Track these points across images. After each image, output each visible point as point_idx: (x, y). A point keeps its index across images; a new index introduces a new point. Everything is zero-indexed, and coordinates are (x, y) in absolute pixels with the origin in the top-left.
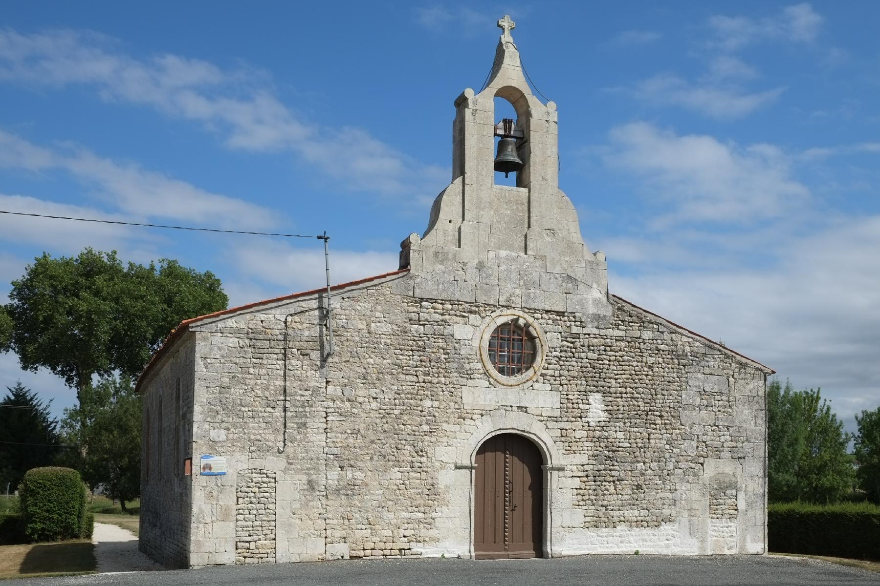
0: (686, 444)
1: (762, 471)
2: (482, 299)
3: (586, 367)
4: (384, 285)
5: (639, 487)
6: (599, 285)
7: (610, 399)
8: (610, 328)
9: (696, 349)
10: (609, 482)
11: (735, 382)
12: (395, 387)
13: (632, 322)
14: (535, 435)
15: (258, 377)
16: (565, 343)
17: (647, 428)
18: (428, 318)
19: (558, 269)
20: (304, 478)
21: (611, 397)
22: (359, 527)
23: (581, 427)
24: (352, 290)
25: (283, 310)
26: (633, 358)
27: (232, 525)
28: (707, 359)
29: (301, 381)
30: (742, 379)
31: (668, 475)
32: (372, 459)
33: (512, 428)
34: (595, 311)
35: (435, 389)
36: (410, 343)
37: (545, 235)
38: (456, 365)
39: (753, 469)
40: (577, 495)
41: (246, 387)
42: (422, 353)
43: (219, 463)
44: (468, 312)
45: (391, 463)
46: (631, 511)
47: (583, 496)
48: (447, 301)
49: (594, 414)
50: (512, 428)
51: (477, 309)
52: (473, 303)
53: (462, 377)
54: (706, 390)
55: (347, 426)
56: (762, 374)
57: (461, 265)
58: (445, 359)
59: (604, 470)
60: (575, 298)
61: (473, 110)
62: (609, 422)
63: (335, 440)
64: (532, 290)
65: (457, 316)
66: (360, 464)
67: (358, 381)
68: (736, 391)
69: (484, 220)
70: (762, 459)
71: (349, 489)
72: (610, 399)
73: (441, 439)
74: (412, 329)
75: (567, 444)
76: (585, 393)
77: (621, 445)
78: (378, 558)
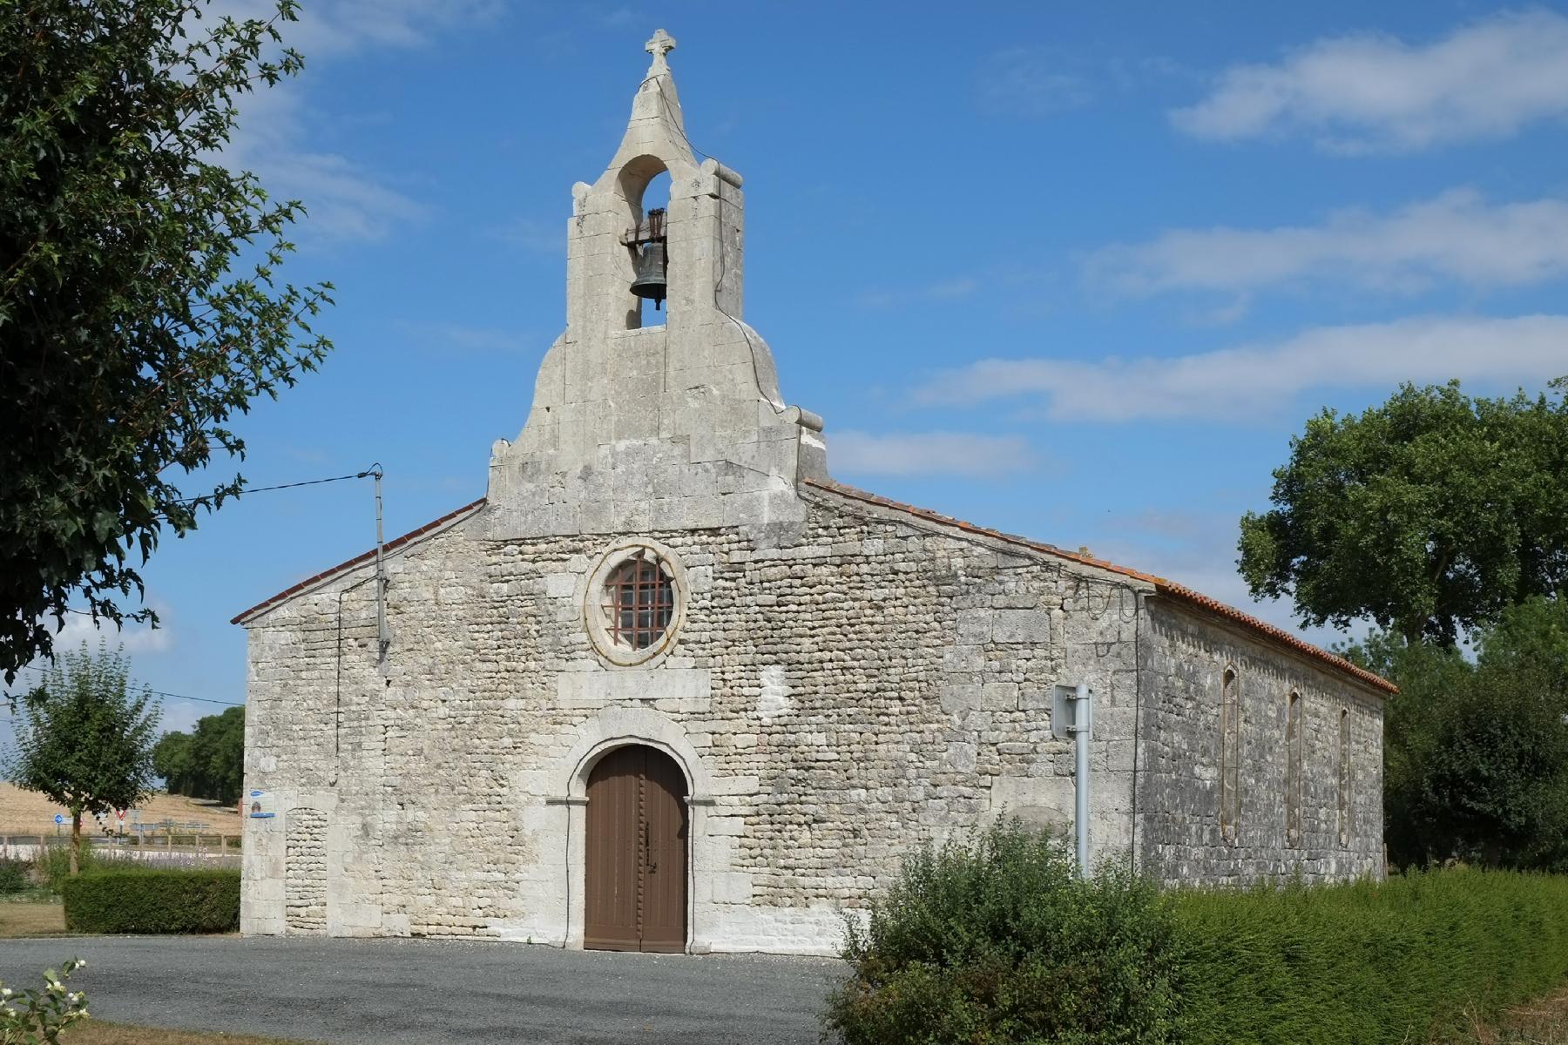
0: (951, 751)
1: (1128, 799)
2: (589, 527)
3: (755, 621)
4: (455, 528)
5: (856, 833)
6: (781, 470)
7: (800, 674)
8: (802, 545)
9: (975, 562)
10: (800, 825)
11: (1066, 619)
12: (468, 682)
13: (845, 527)
14: (668, 745)
15: (309, 683)
16: (721, 583)
17: (872, 724)
18: (513, 570)
19: (709, 454)
20: (358, 820)
21: (801, 670)
22: (421, 891)
23: (745, 728)
24: (415, 543)
25: (338, 586)
26: (846, 594)
27: (281, 883)
28: (1001, 578)
29: (357, 683)
30: (1082, 609)
31: (914, 811)
32: (437, 791)
33: (631, 736)
34: (774, 518)
35: (520, 681)
36: (489, 612)
37: (689, 400)
38: (550, 640)
39: (1105, 795)
40: (740, 847)
41: (298, 698)
42: (503, 626)
43: (268, 800)
44: (570, 552)
45: (461, 797)
46: (840, 878)
47: (751, 849)
48: (540, 538)
49: (769, 704)
50: (631, 736)
51: (581, 545)
52: (577, 536)
53: (558, 658)
54: (996, 639)
55: (408, 744)
56: (1131, 594)
57: (559, 477)
58: (538, 631)
59: (789, 803)
60: (738, 499)
61: (579, 216)
62: (798, 716)
63: (393, 765)
64: (667, 499)
65: (554, 561)
66: (423, 799)
67: (423, 677)
68: (1066, 635)
69: (592, 396)
70: (1129, 775)
71: (408, 837)
72: (800, 674)
73: (528, 759)
74: (492, 591)
75: (722, 759)
76: (753, 668)
77: (820, 756)
78: (444, 937)
